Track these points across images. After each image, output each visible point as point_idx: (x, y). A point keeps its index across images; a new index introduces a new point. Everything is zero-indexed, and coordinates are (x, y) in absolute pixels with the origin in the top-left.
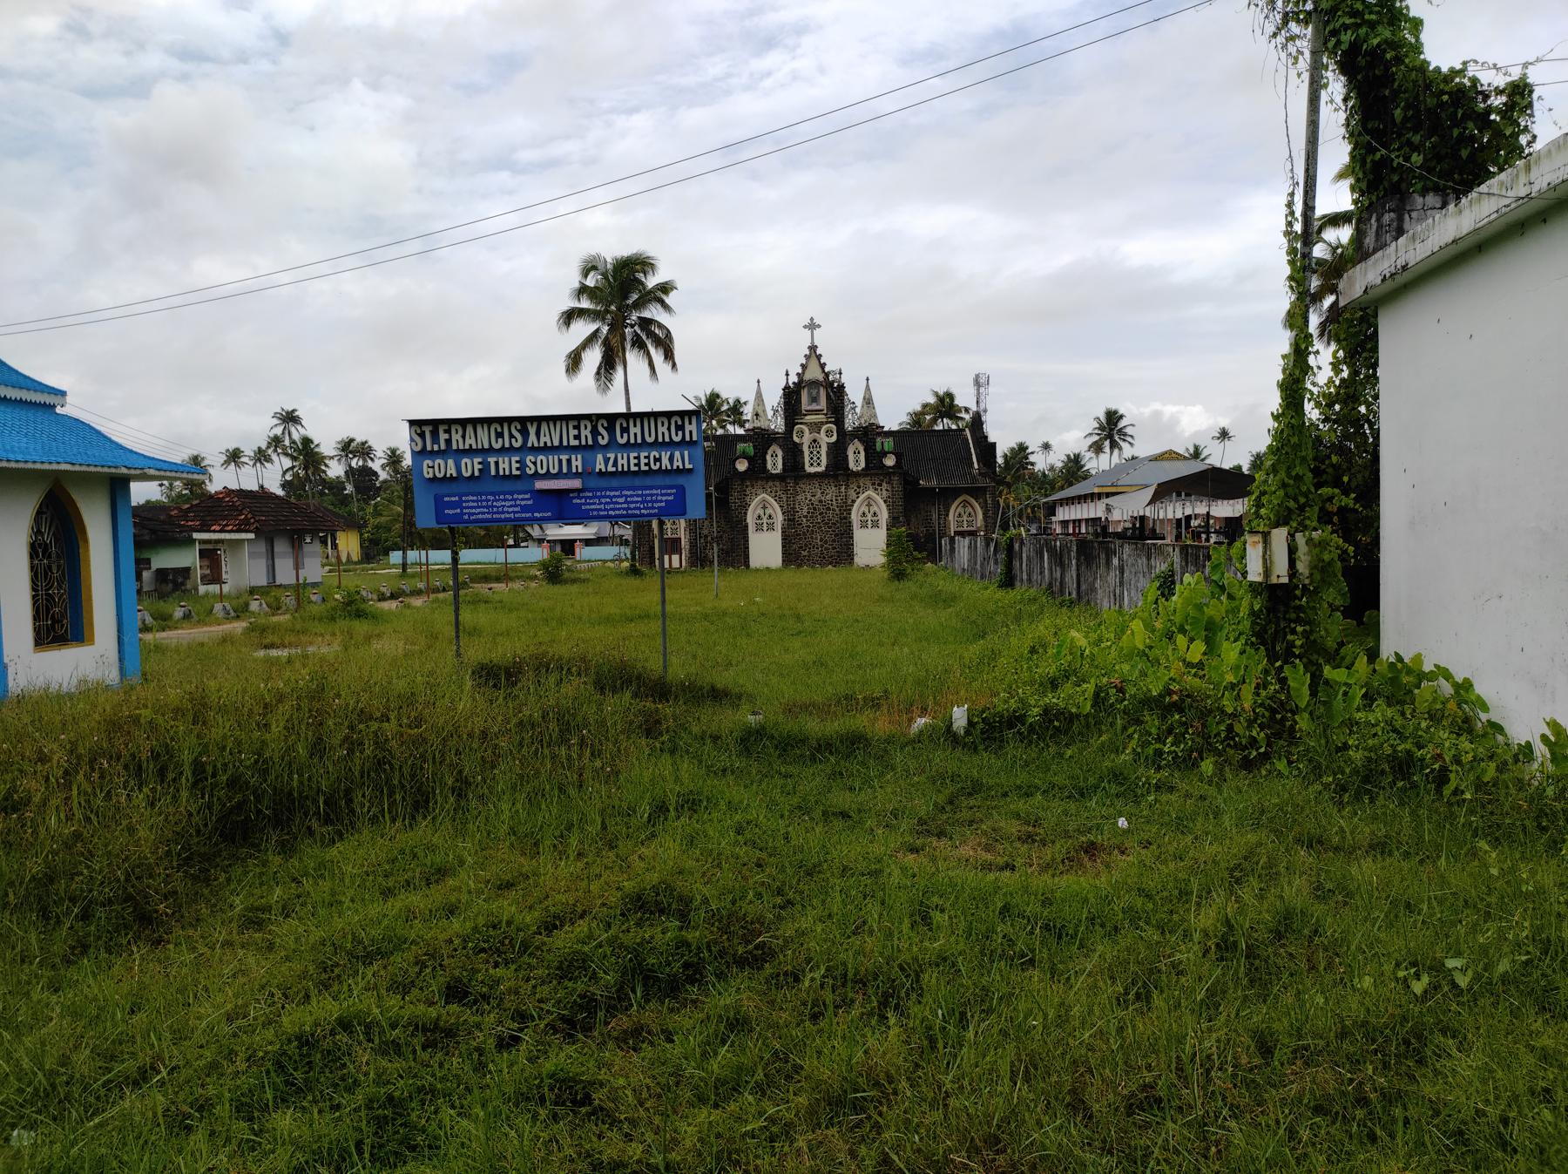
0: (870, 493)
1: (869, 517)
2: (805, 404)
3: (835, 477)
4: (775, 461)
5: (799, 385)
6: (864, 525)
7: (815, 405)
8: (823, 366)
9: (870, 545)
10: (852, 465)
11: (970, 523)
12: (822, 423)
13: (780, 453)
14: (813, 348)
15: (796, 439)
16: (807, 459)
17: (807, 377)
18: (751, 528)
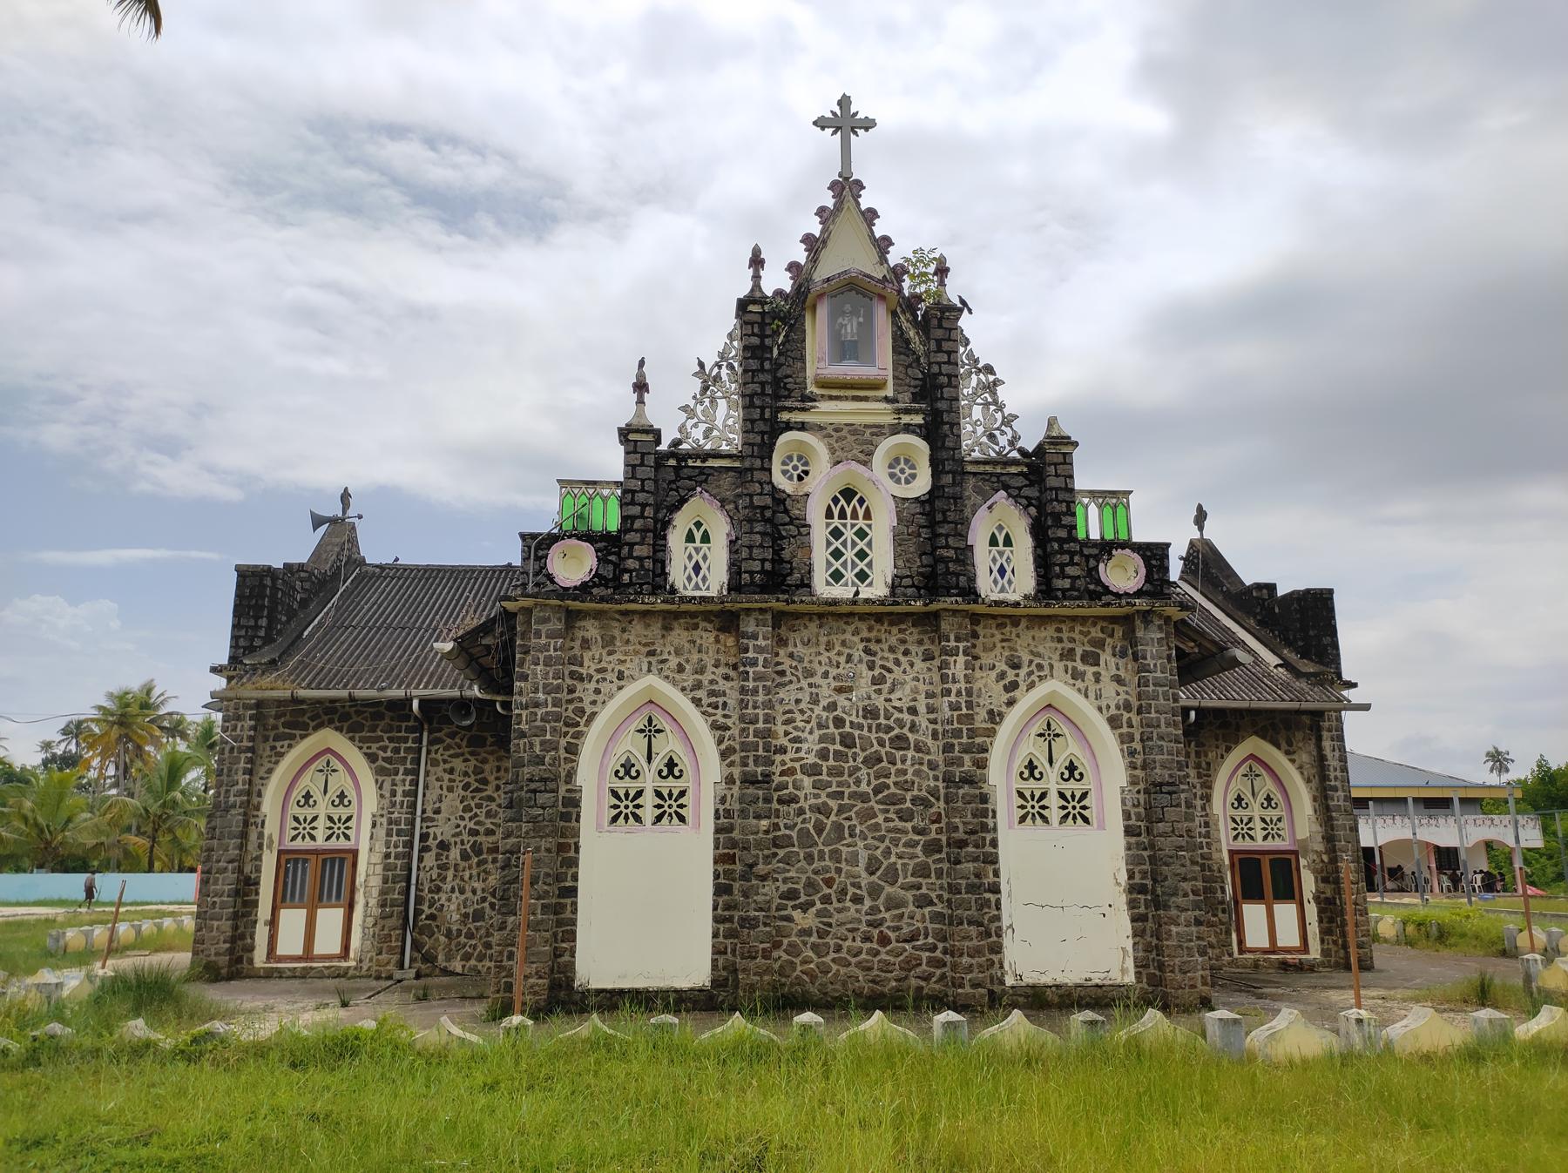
0: (1056, 687)
1: (1052, 781)
3: (928, 622)
4: (700, 551)
5: (802, 296)
6: (1033, 810)
7: (846, 362)
8: (884, 244)
10: (986, 585)
12: (879, 431)
13: (720, 528)
14: (846, 187)
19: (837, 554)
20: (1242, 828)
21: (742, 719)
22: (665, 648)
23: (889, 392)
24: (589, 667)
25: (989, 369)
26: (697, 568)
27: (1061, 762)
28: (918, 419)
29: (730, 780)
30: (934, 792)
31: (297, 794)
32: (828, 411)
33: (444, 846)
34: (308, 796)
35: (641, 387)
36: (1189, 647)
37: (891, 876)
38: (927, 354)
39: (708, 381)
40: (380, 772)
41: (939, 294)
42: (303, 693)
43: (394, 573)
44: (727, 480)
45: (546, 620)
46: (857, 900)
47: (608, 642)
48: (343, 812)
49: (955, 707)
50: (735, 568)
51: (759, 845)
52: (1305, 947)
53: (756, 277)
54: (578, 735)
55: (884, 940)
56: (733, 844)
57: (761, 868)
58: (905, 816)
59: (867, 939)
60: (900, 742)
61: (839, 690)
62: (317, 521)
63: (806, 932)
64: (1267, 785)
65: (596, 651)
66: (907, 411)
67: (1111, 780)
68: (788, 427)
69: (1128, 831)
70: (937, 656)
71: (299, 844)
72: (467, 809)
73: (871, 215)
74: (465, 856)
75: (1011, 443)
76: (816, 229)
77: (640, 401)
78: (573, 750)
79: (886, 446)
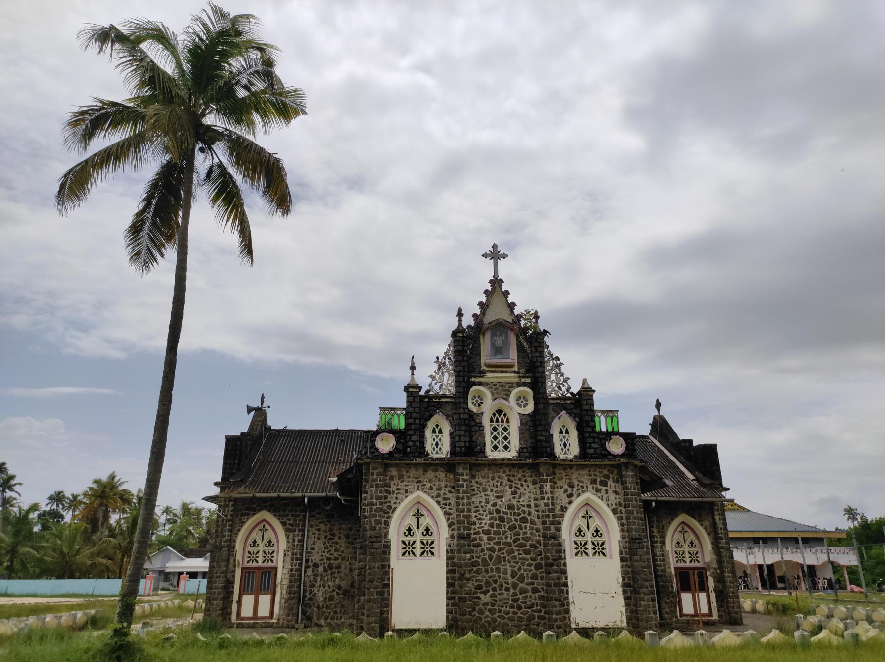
0: (589, 495)
1: (589, 537)
2: (486, 355)
3: (534, 468)
4: (439, 440)
5: (479, 328)
6: (581, 549)
7: (500, 359)
8: (512, 306)
9: (596, 589)
10: (558, 451)
11: (694, 556)
12: (512, 385)
13: (447, 428)
14: (496, 282)
15: (471, 407)
16: (488, 439)
17: (489, 318)
18: (396, 549)
19: (495, 438)
20: (680, 557)
21: (457, 510)
22: (424, 479)
23: (516, 369)
24: (393, 488)
25: (557, 359)
26: (437, 444)
27: (592, 529)
28: (528, 380)
29: (452, 537)
30: (539, 542)
31: (250, 541)
32: (491, 377)
33: (316, 565)
34: (255, 542)
35: (413, 368)
36: (646, 477)
37: (521, 579)
38: (532, 352)
39: (441, 365)
40: (287, 530)
41: (536, 327)
42: (258, 495)
43: (285, 433)
44: (449, 407)
45: (375, 468)
46: (507, 589)
47: (401, 477)
48: (270, 549)
49: (546, 505)
50: (453, 444)
51: (466, 565)
52: (710, 614)
53: (460, 321)
54: (389, 517)
55: (519, 608)
56: (454, 565)
57: (467, 575)
58: (527, 552)
59: (512, 607)
60: (524, 520)
61: (498, 497)
62: (250, 410)
63: (486, 604)
64: (691, 537)
65: (396, 481)
66: (524, 377)
67: (614, 536)
68: (474, 384)
69: (622, 560)
70: (539, 482)
71: (251, 564)
72: (326, 548)
73: (506, 294)
74: (325, 570)
75: (568, 390)
76: (484, 300)
77: (413, 374)
78: (387, 524)
79: (515, 392)
